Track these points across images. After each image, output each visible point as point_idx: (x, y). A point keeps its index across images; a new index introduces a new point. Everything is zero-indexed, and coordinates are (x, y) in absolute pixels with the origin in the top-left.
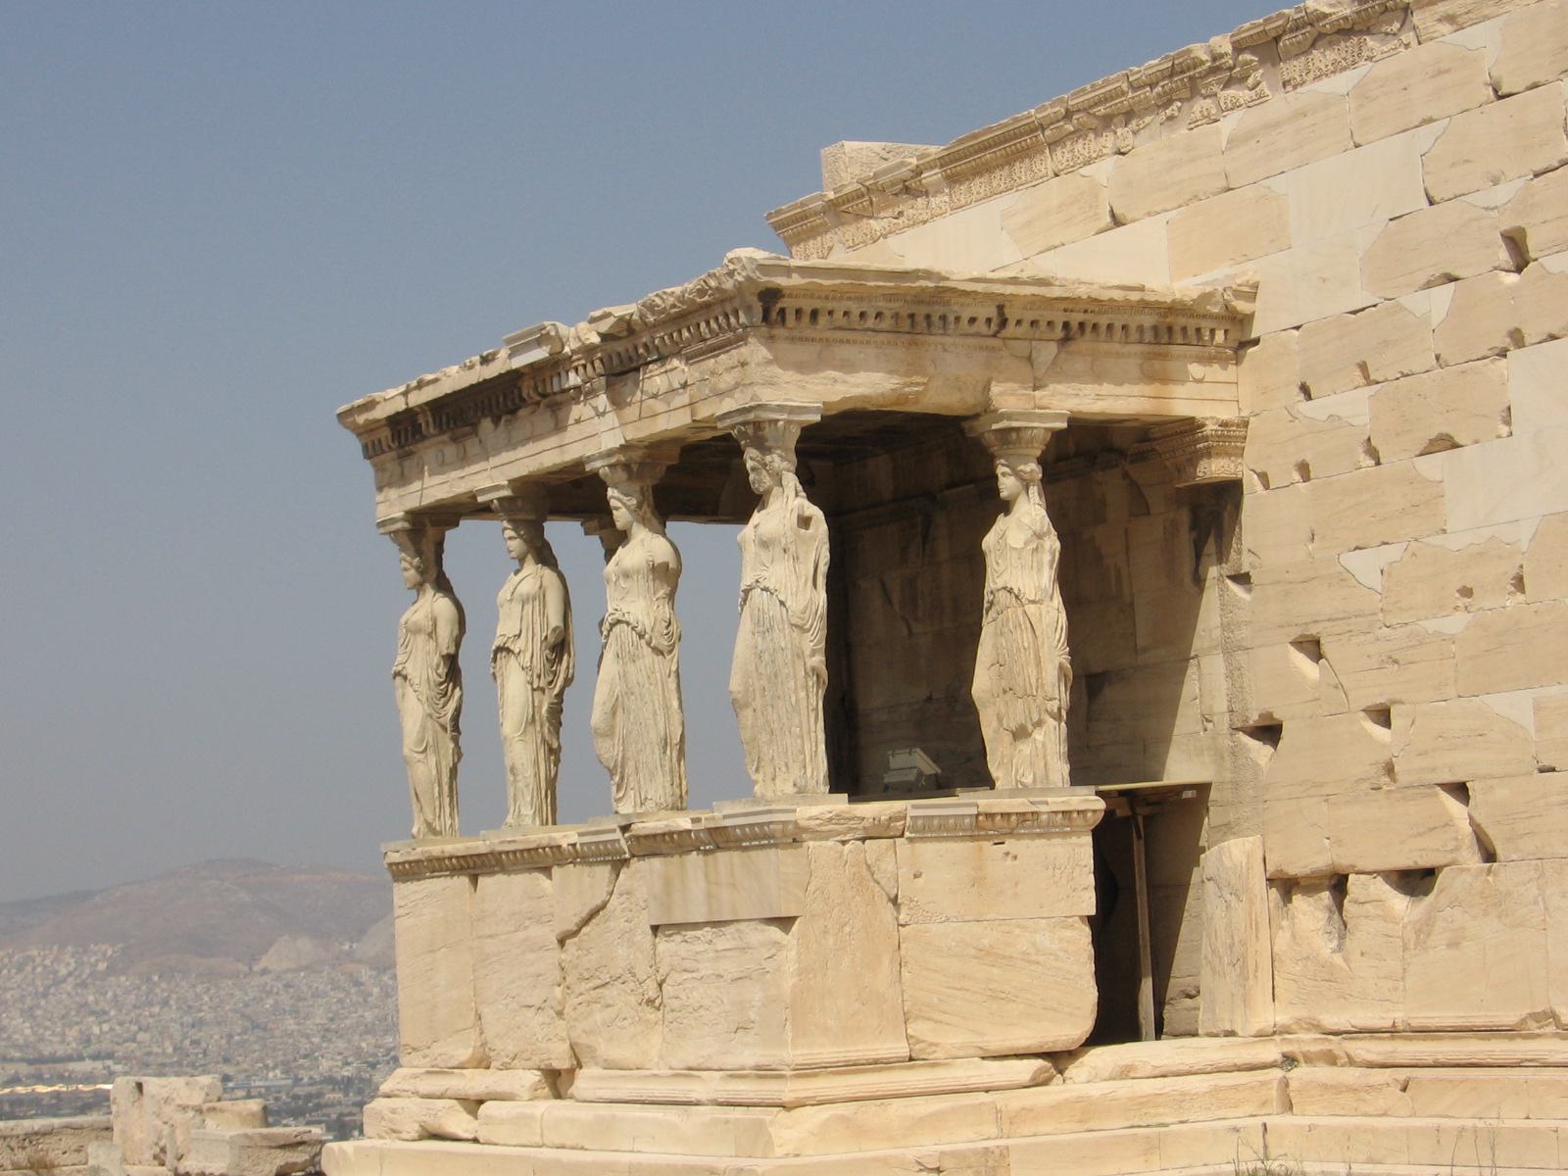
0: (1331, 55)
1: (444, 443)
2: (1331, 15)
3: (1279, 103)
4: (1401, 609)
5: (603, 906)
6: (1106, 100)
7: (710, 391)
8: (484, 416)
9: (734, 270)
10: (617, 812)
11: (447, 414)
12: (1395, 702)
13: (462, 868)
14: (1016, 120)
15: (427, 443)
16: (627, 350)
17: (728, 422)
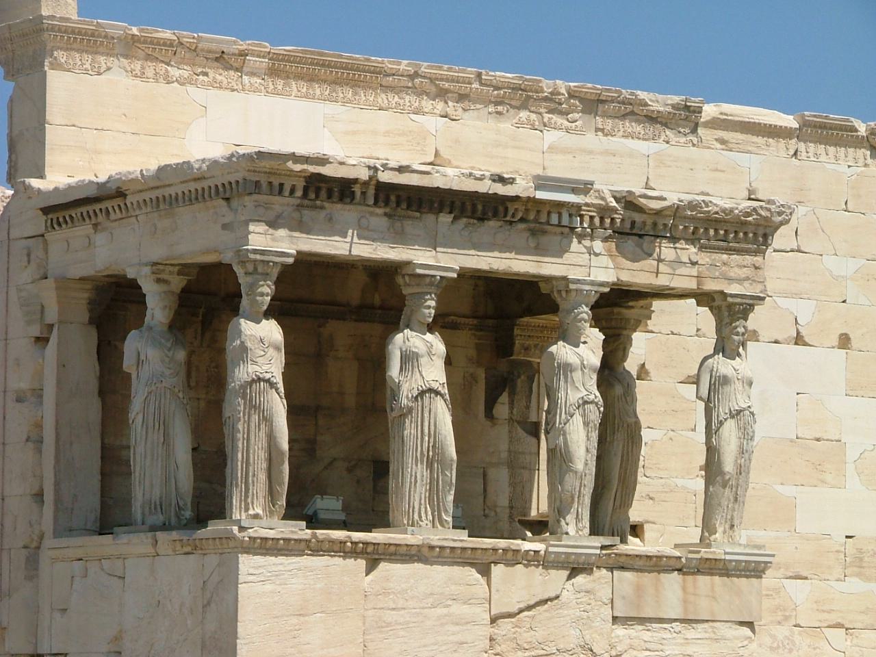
0: (638, 128)
1: (372, 214)
2: (650, 105)
3: (591, 140)
4: (659, 469)
5: (557, 597)
6: (453, 81)
7: (720, 274)
8: (451, 212)
9: (785, 212)
10: (567, 533)
11: (398, 197)
12: (648, 522)
13: (362, 553)
14: (368, 60)
15: (348, 207)
16: (644, 223)
17: (738, 300)
